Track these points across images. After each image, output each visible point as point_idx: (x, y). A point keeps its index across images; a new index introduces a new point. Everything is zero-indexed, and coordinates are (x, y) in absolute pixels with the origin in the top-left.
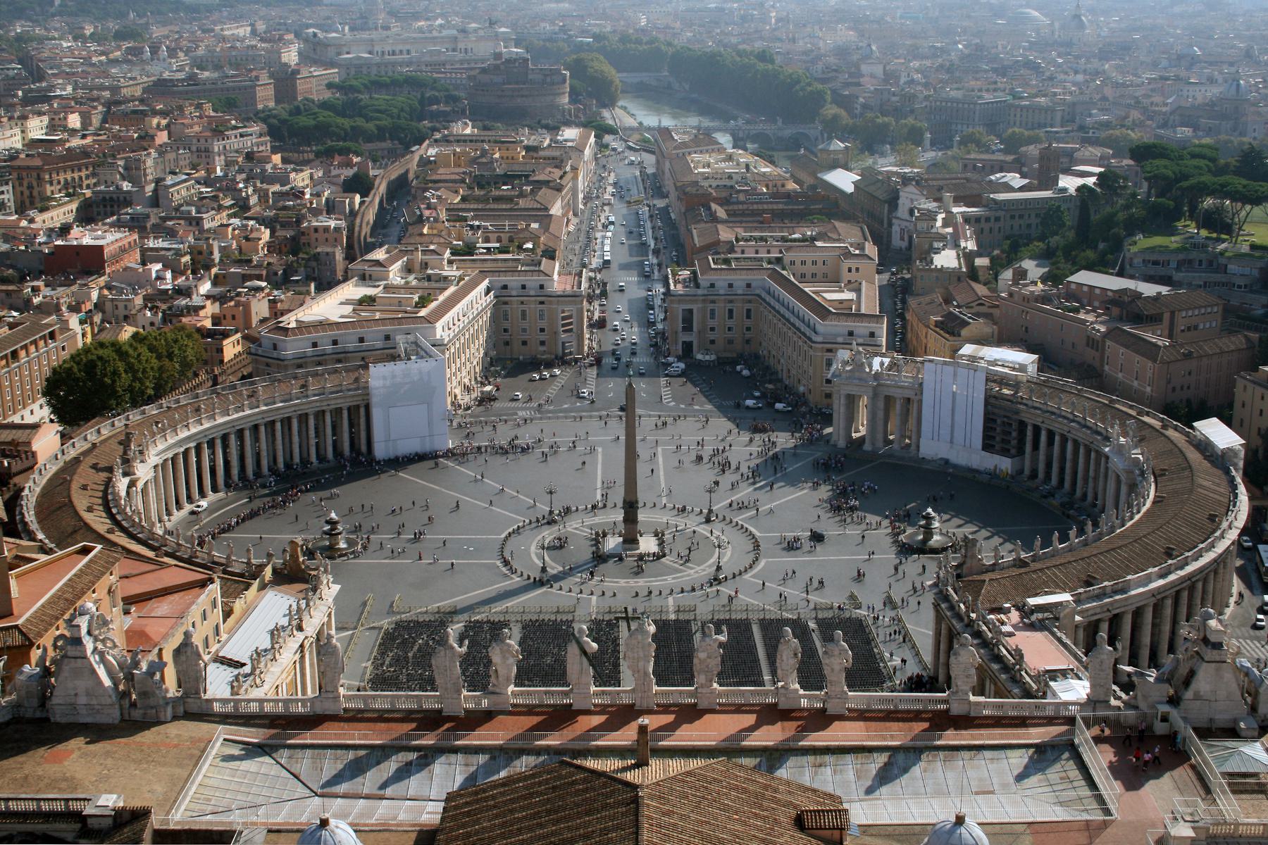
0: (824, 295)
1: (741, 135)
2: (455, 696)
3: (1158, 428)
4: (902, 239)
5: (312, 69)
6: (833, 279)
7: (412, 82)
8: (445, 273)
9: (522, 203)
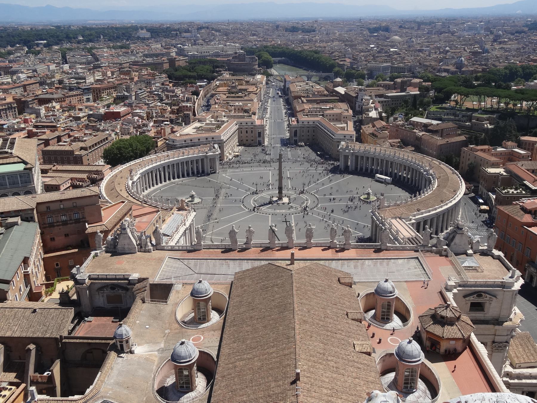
4: (359, 108)
7: (211, 62)
8: (223, 120)
9: (246, 98)
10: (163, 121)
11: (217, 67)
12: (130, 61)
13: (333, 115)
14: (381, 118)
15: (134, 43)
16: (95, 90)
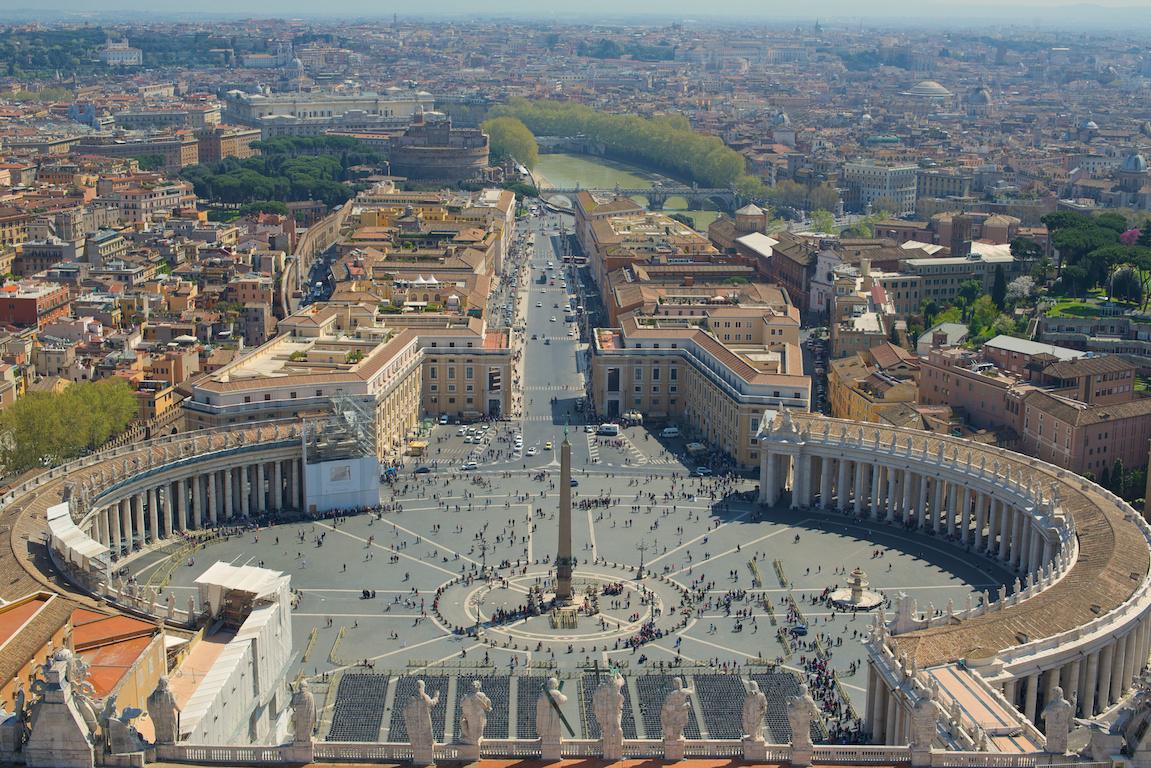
2: (426, 746)
3: (1079, 489)
5: (236, 129)
6: (755, 339)
7: (336, 144)
8: (375, 331)
9: (448, 263)
10: (175, 333)
11: (357, 161)
12: (73, 137)
13: (738, 325)
14: (894, 337)
15: (89, 83)
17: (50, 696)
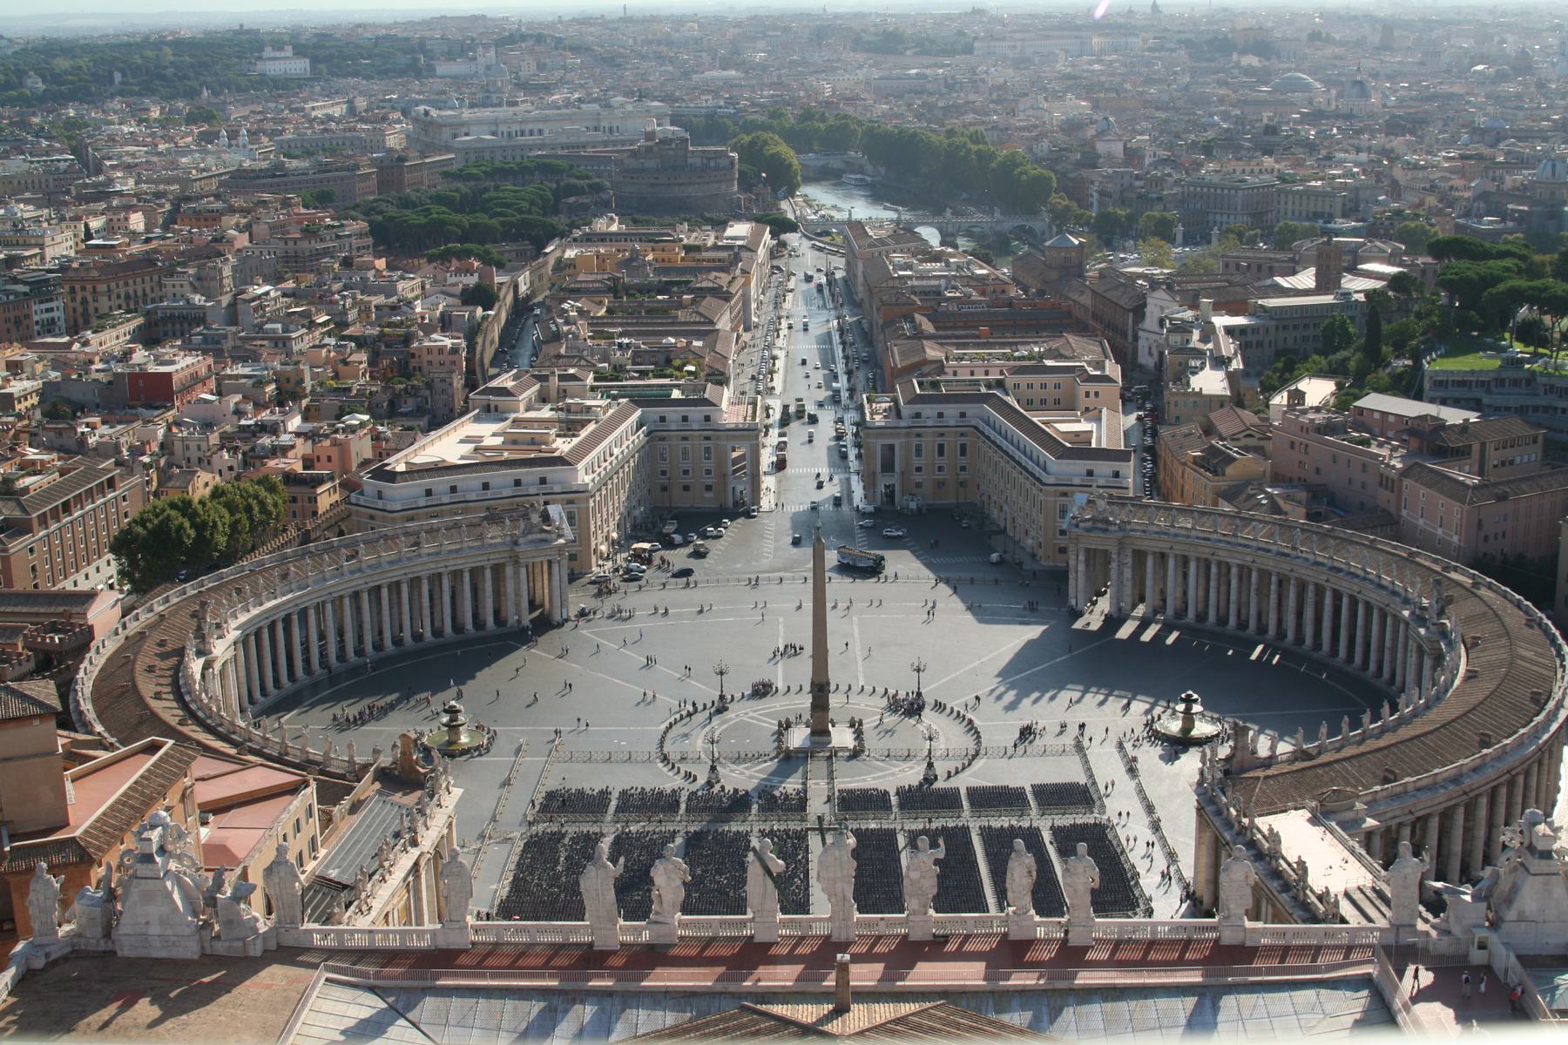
0: (1056, 425)
1: (950, 229)
2: (610, 926)
3: (1469, 586)
4: (1150, 354)
6: (1065, 405)
7: (546, 169)
9: (682, 315)
16: (78, 287)
17: (143, 870)
